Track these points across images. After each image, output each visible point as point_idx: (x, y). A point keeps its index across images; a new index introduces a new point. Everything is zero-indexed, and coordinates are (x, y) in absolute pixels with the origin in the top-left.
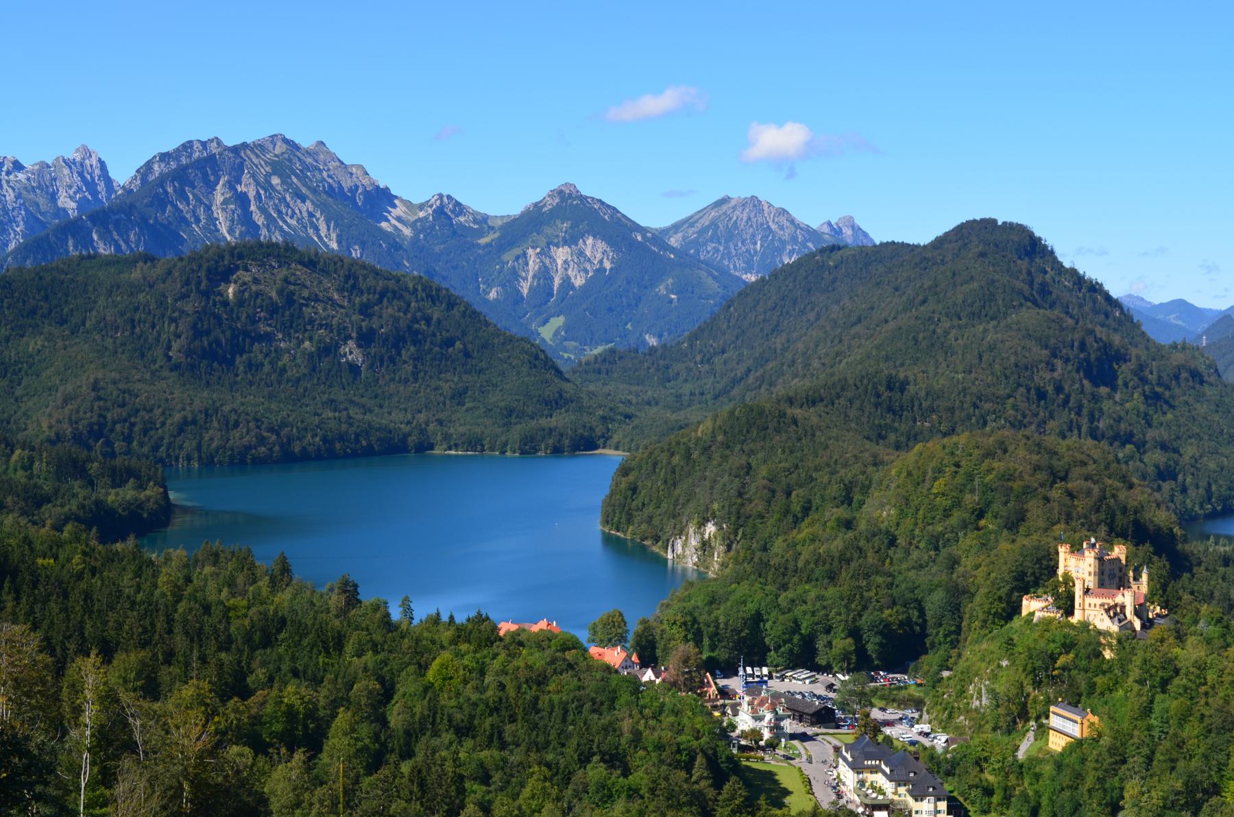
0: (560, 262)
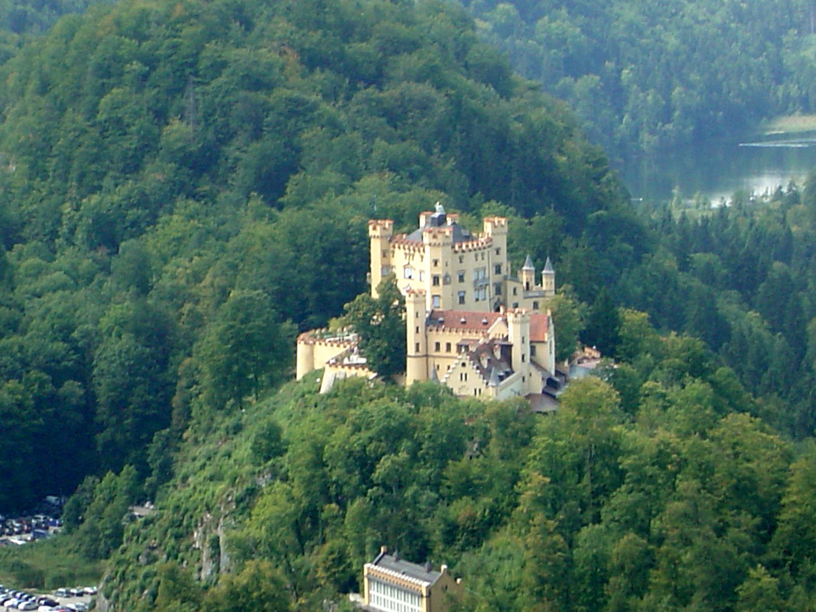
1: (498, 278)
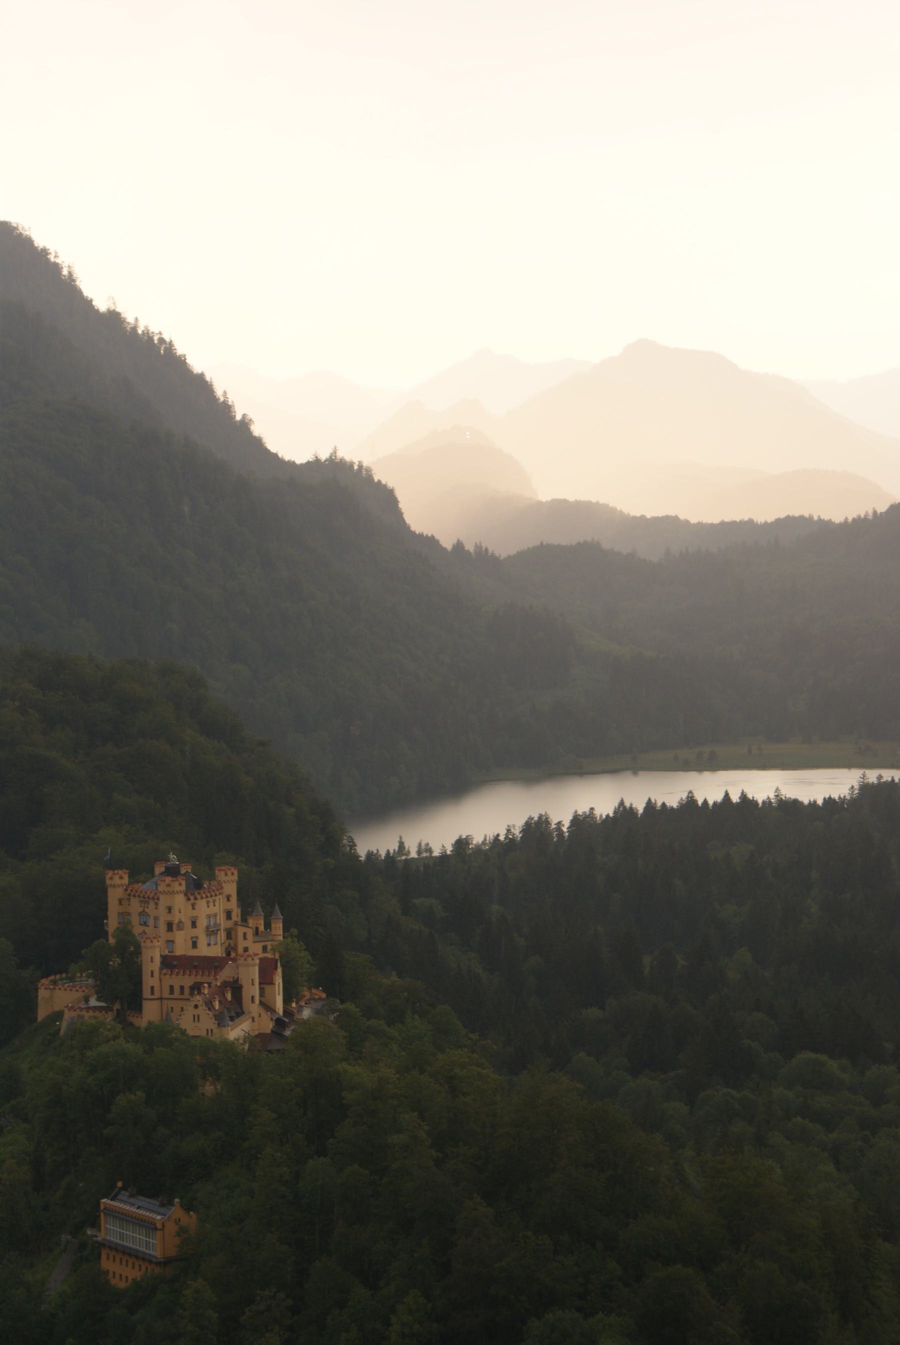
1: (230, 924)
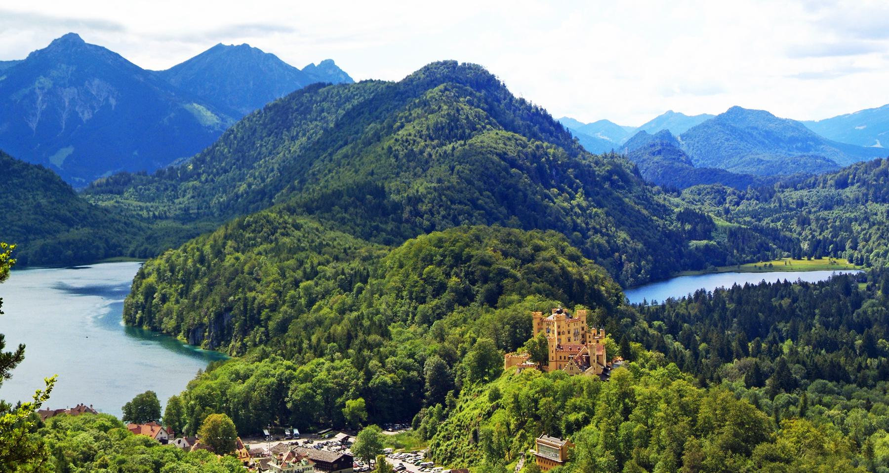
0: (67, 100)
1: (583, 332)
